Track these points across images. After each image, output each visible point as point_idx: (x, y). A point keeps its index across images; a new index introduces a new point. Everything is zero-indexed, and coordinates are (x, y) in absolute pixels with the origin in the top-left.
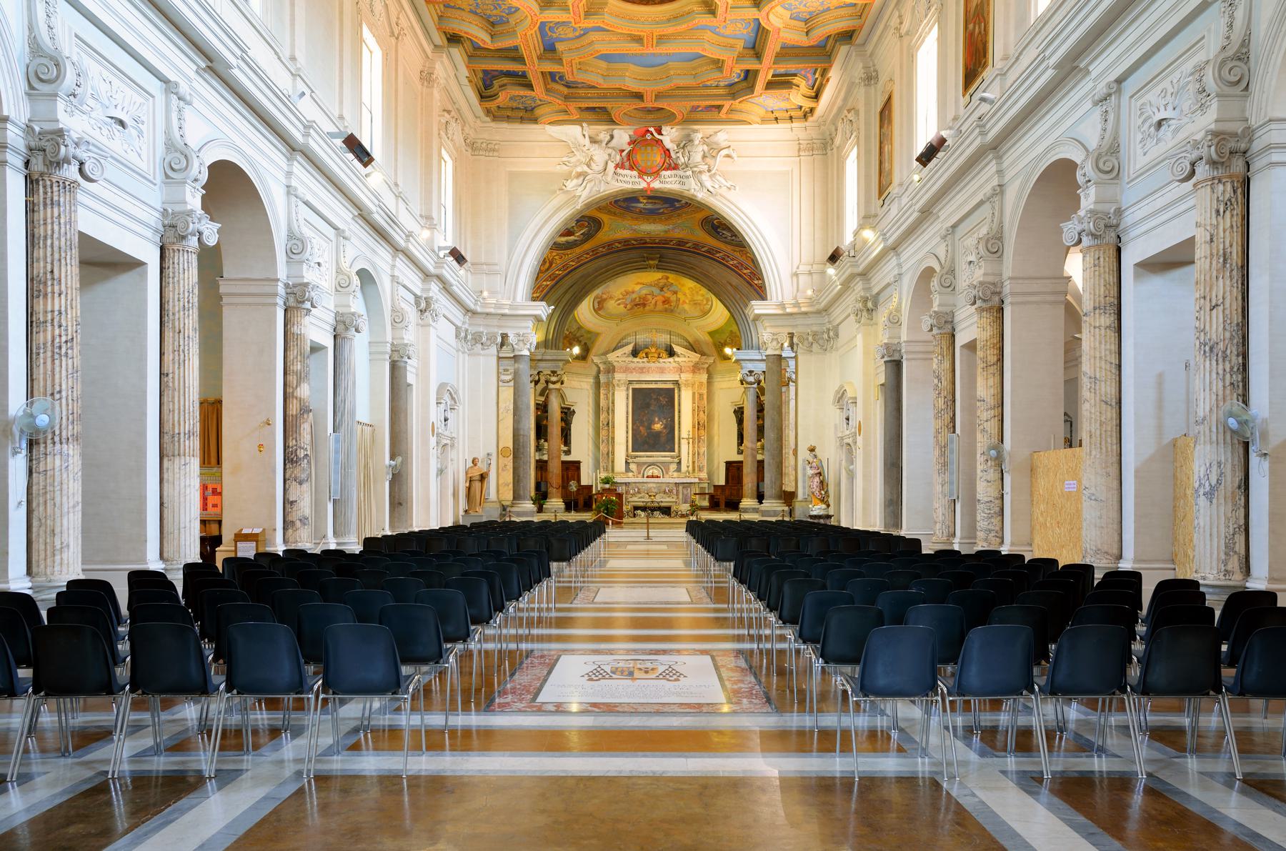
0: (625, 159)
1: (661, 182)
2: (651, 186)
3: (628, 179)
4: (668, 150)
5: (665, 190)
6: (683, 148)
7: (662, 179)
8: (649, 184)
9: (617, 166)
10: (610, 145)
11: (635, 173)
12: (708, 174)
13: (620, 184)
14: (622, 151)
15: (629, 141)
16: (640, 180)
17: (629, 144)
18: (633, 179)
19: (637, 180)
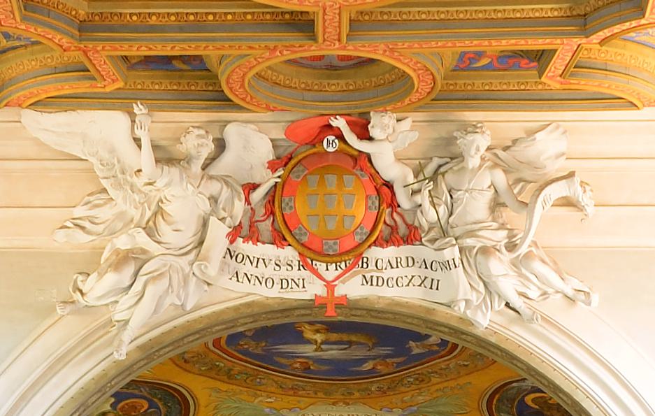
0: (261, 212)
1: (367, 281)
2: (341, 290)
3: (269, 271)
4: (389, 185)
5: (381, 305)
6: (434, 178)
7: (371, 272)
8: (330, 286)
9: (235, 233)
10: (214, 170)
11: (289, 253)
12: (507, 256)
13: (245, 287)
14: (251, 187)
15: (271, 157)
16: (305, 273)
17: (273, 166)
18: (284, 273)
19: (296, 274)
